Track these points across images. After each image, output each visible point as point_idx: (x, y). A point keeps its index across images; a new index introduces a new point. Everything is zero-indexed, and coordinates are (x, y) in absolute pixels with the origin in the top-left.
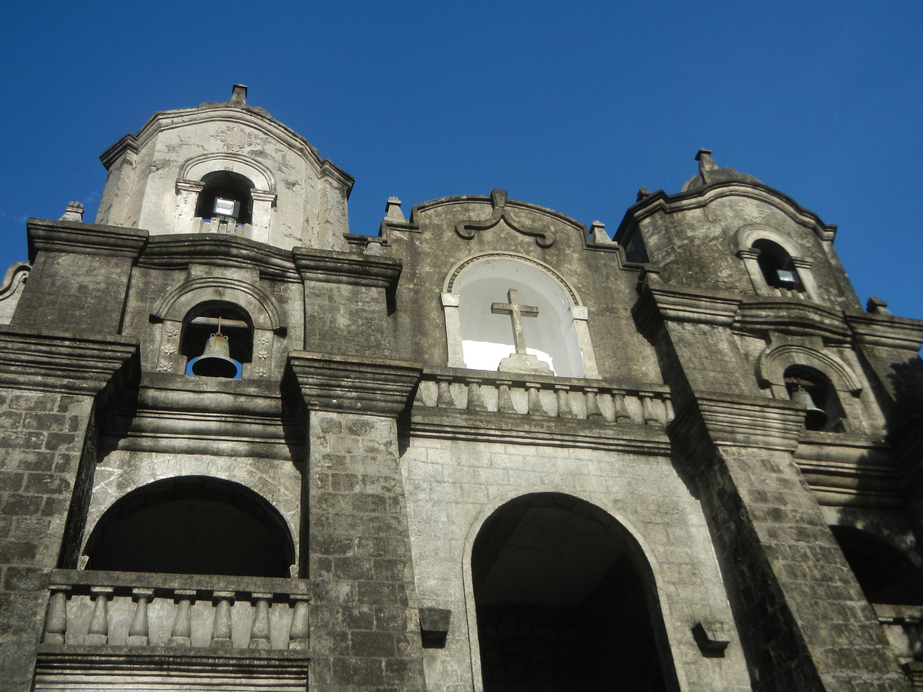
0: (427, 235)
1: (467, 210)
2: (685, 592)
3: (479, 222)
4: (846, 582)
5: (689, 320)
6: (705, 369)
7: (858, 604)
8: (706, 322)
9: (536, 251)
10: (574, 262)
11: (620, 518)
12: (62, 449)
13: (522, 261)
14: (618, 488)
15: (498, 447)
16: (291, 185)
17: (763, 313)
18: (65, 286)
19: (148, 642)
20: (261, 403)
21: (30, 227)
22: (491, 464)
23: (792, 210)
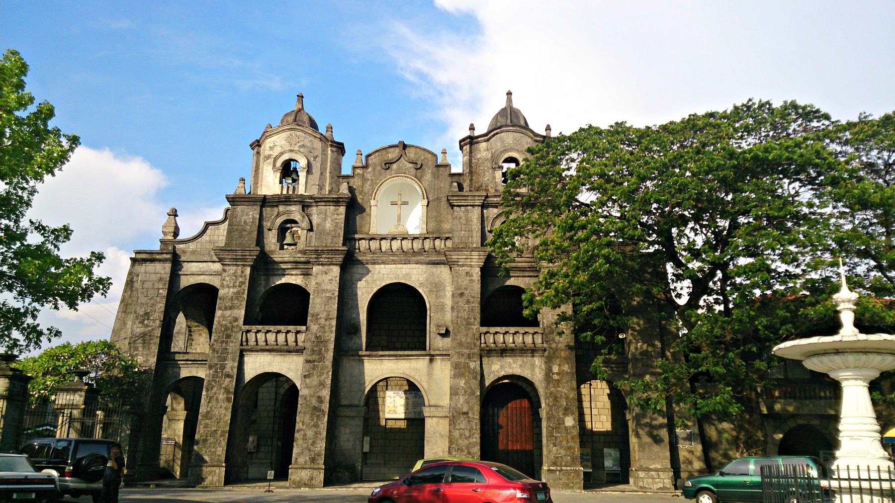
0: (370, 170)
1: (388, 153)
2: (436, 316)
3: (393, 159)
4: (475, 319)
5: (463, 206)
6: (461, 231)
7: (476, 327)
8: (470, 206)
9: (413, 171)
10: (428, 176)
11: (420, 290)
12: (243, 286)
13: (406, 179)
14: (422, 279)
15: (382, 266)
16: (315, 158)
17: (495, 199)
18: (240, 222)
19: (267, 344)
20: (302, 259)
21: (227, 198)
22: (379, 273)
23: (532, 135)
